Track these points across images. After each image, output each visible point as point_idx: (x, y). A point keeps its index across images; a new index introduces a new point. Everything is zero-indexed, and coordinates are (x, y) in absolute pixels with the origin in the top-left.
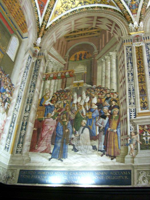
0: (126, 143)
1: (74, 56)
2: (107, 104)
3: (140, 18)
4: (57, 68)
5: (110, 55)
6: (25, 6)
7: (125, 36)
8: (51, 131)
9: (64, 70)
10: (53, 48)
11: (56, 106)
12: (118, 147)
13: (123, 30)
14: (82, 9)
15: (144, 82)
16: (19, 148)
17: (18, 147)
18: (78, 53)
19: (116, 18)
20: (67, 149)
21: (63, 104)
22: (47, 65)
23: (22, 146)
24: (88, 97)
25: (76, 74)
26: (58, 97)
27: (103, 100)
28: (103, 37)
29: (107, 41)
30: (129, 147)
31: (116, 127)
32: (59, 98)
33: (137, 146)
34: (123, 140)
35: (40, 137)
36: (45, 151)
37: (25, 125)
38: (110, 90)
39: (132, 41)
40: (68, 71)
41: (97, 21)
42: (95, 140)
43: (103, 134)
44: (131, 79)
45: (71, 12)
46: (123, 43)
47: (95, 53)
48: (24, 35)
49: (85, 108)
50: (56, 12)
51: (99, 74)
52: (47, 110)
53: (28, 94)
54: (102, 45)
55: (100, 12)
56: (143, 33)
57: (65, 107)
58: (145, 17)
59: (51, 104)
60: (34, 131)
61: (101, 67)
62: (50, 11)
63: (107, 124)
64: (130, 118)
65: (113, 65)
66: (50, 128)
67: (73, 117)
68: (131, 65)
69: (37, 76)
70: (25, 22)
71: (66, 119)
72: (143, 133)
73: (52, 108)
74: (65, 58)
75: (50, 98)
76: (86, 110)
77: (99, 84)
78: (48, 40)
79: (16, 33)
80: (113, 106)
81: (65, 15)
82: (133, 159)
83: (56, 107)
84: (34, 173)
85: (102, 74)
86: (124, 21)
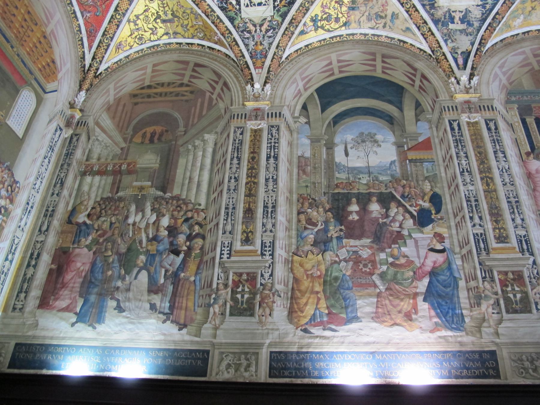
0: (207, 302)
1: (140, 133)
3: (267, 78)
4: (108, 155)
5: (204, 140)
6: (55, 31)
7: (237, 107)
9: (119, 159)
10: (105, 112)
11: (96, 226)
12: (193, 308)
13: (235, 96)
14: (169, 44)
15: (253, 195)
16: (18, 301)
18: (149, 130)
19: (228, 71)
20: (106, 307)
21: (109, 224)
22: (90, 146)
23: (25, 297)
24: (155, 214)
25: (140, 168)
27: (180, 221)
28: (199, 104)
29: (204, 112)
30: (211, 309)
31: (195, 273)
33: (225, 309)
35: (61, 281)
36: (67, 309)
37: (36, 259)
38: (194, 205)
39: (245, 117)
40: (127, 161)
41: (194, 70)
42: (156, 293)
43: (170, 283)
44: (233, 188)
45: (149, 48)
48: (50, 87)
50: (120, 45)
51: (180, 172)
53: (49, 198)
54: (194, 118)
55: (201, 55)
56: (268, 105)
57: (113, 229)
58: (276, 75)
59: (88, 222)
60: (51, 271)
61: (185, 160)
62: (107, 43)
63: (180, 265)
64: (221, 258)
67: (123, 249)
68: (237, 162)
69: (69, 165)
70: (53, 62)
71: (112, 252)
72: (239, 287)
74: (125, 136)
75: (87, 210)
76: (148, 237)
77: (176, 191)
79: (31, 83)
80: (194, 233)
81: (138, 52)
82: (214, 331)
83: (97, 228)
84: (42, 349)
85: (185, 174)
86: (241, 78)
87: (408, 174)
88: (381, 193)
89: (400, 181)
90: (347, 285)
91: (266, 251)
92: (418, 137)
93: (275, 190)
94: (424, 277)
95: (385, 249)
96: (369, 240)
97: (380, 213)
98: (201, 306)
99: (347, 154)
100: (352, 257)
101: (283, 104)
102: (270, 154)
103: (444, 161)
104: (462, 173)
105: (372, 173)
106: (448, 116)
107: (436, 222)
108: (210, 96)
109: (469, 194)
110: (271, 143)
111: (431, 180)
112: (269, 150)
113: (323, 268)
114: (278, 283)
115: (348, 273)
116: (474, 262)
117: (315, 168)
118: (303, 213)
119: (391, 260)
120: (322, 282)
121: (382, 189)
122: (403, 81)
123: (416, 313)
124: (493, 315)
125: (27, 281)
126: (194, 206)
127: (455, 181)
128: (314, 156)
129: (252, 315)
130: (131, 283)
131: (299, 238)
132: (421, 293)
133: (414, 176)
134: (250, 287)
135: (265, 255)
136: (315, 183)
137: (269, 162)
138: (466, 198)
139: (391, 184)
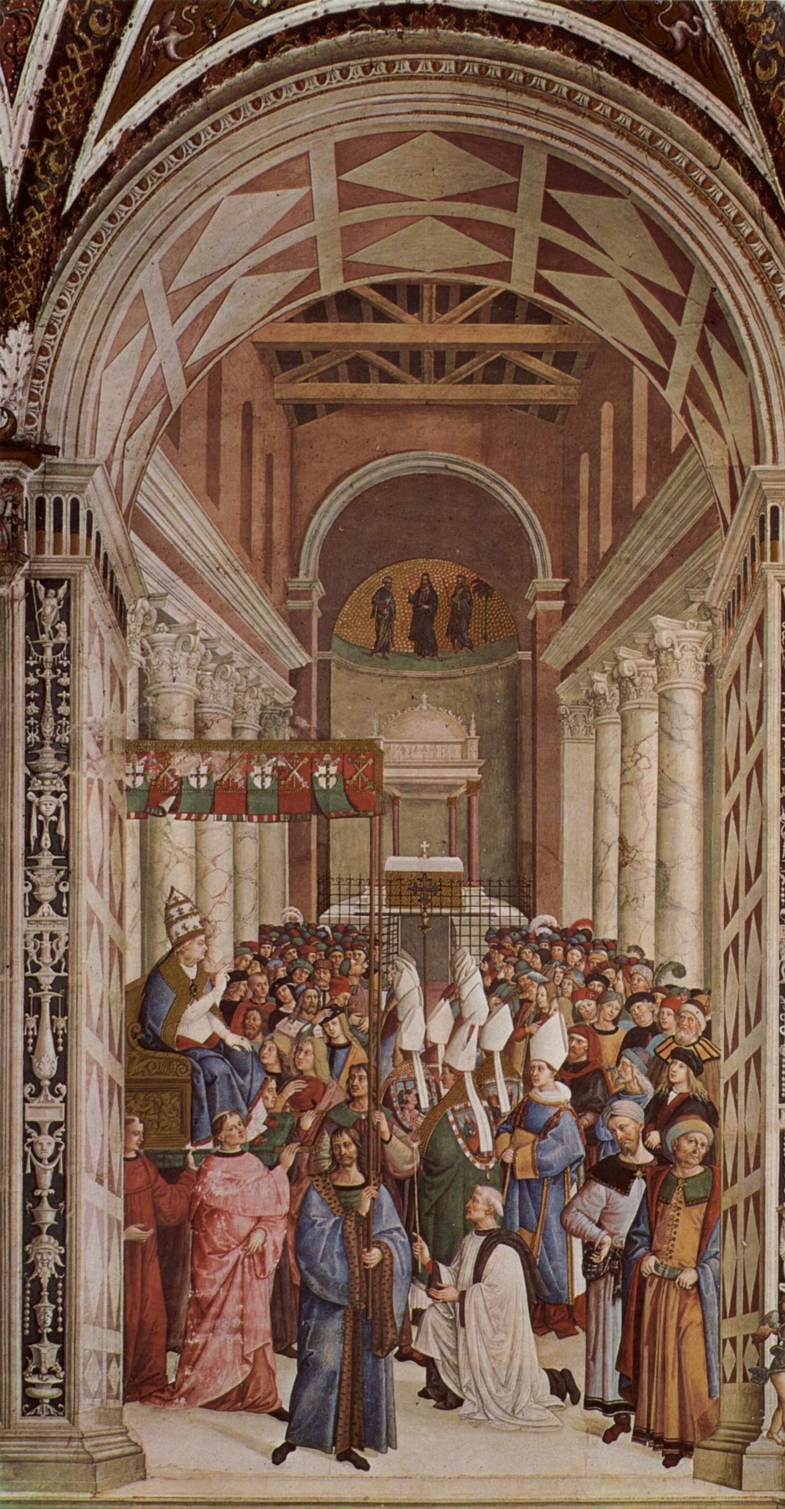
2: (634, 1077)
4: (238, 709)
5: (659, 651)
8: (262, 1255)
10: (158, 454)
11: (270, 1059)
12: (704, 1389)
16: (37, 1371)
17: (32, 1368)
21: (323, 1050)
22: (136, 653)
23: (61, 1357)
24: (506, 1008)
25: (403, 786)
26: (281, 982)
32: (285, 992)
34: (733, 1341)
37: (54, 1201)
38: (659, 971)
43: (610, 1293)
46: (762, 539)
47: (540, 604)
49: (489, 1100)
52: (209, 1085)
59: (232, 1040)
60: (131, 1247)
63: (636, 1223)
65: (680, 748)
66: (253, 1230)
69: (65, 753)
71: (361, 1170)
73: (243, 1074)
74: (292, 604)
78: (104, 353)
80: (673, 1096)
83: (276, 1069)
98: (733, 1379)
108: (653, 395)
125: (45, 1293)
126: (657, 979)
130: (463, 1295)
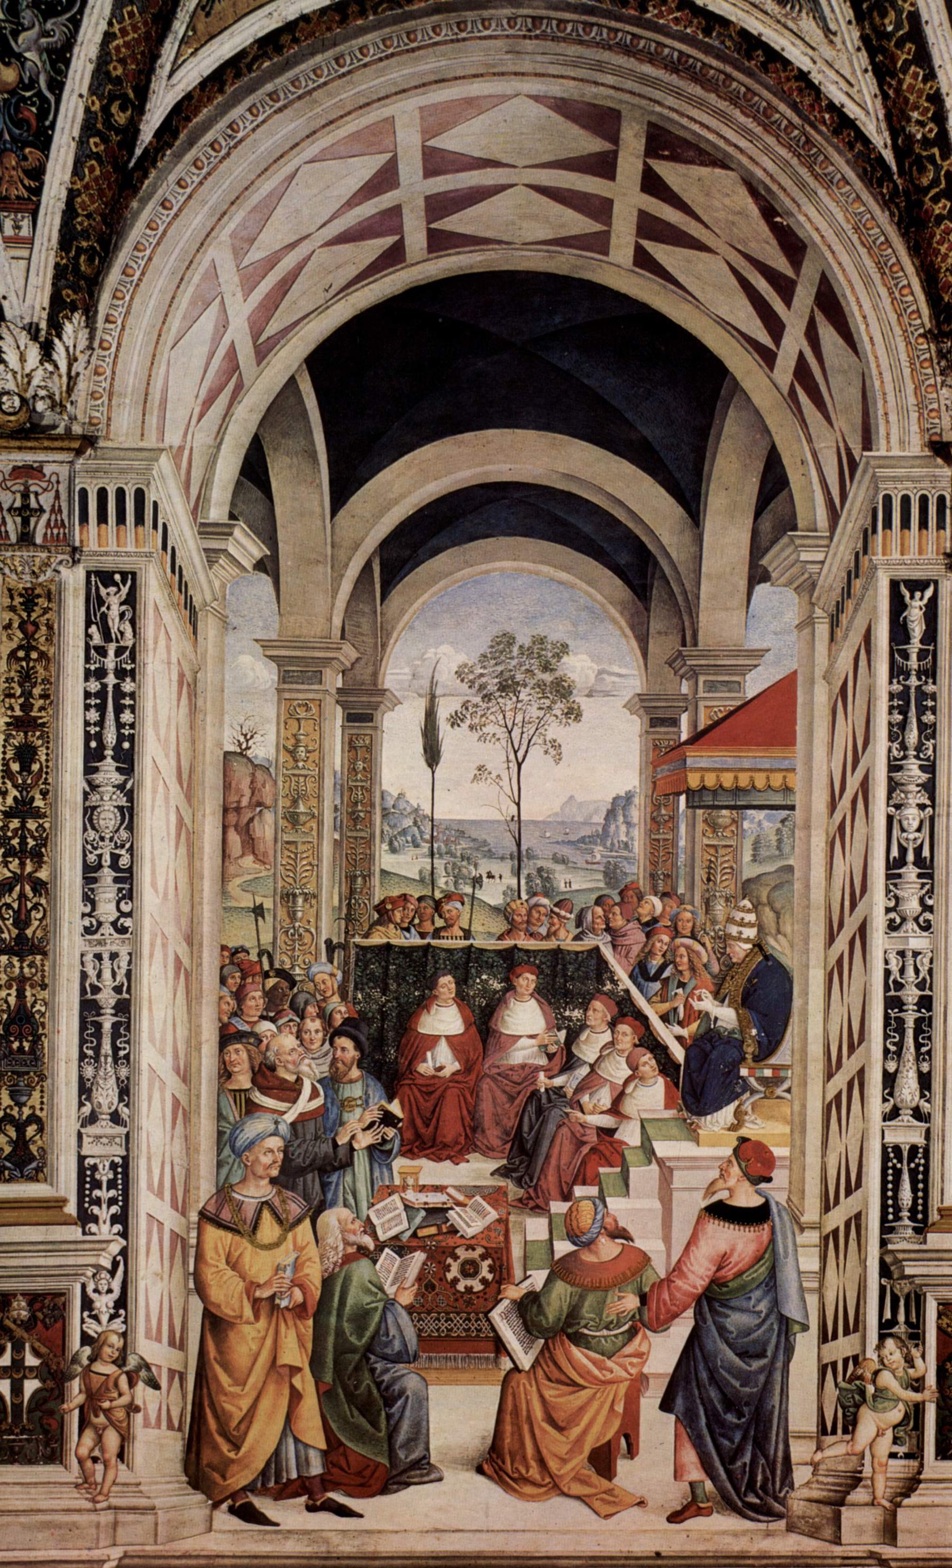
87: (674, 865)
88: (557, 952)
89: (640, 897)
90: (397, 1345)
91: (98, 1202)
92: (743, 670)
93: (128, 922)
94: (676, 1315)
95: (547, 1204)
96: (494, 1165)
97: (543, 1047)
99: (432, 755)
100: (421, 1233)
101: (151, 442)
102: (99, 737)
103: (833, 806)
104: (894, 866)
105: (530, 857)
106: (896, 555)
107: (753, 1092)
109: (902, 971)
110: (101, 673)
111: (764, 899)
112: (93, 716)
113: (314, 1274)
114: (148, 1336)
115: (406, 1298)
116: (863, 1262)
117: (293, 819)
118: (240, 1036)
119: (563, 1247)
120: (311, 1331)
121: (562, 934)
122: (725, 324)
123: (632, 1452)
124: (892, 1462)
127: (861, 907)
128: (292, 753)
129: (55, 1456)
131: (227, 1151)
132: (658, 1376)
133: (700, 874)
134: (43, 1350)
135: (95, 1220)
136: (295, 896)
137: (99, 778)
138: (887, 988)
139: (599, 910)
